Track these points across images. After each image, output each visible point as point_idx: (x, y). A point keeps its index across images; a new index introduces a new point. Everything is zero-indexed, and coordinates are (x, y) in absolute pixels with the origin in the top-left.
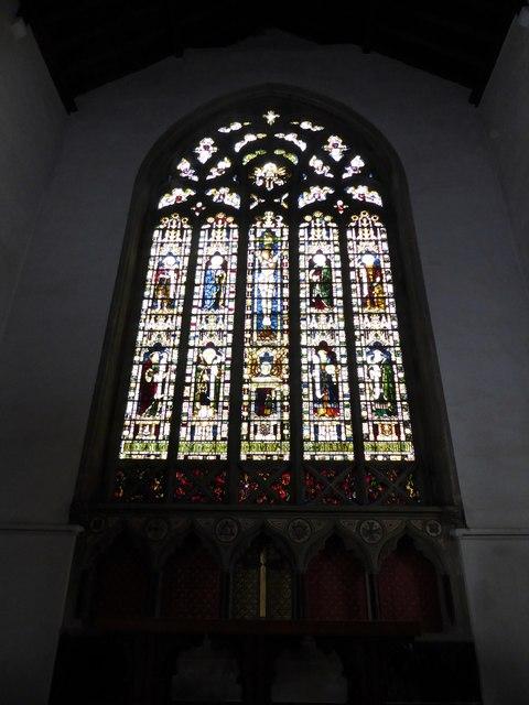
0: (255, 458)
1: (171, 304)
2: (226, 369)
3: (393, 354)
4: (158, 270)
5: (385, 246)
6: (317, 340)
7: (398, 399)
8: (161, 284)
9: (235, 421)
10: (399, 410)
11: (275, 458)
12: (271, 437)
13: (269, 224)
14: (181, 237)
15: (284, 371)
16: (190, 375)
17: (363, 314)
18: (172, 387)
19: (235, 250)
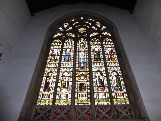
0: (80, 104)
1: (55, 61)
2: (71, 78)
3: (119, 73)
4: (52, 52)
5: (113, 46)
6: (97, 70)
7: (122, 85)
8: (53, 55)
9: (73, 93)
10: (123, 89)
11: (86, 104)
12: (84, 98)
13: (82, 41)
14: (59, 44)
15: (88, 78)
16: (60, 80)
17: (109, 62)
18: (55, 83)
19: (73, 47)
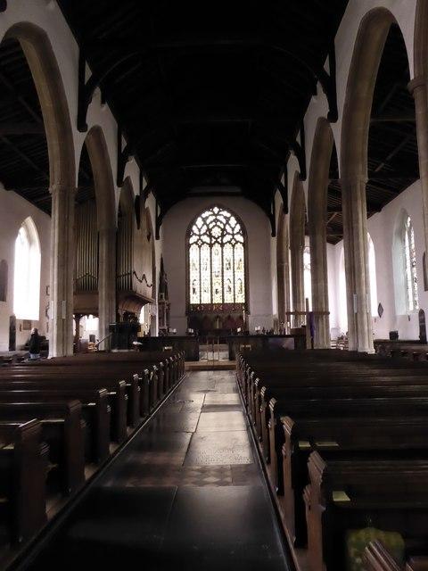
9: (212, 295)
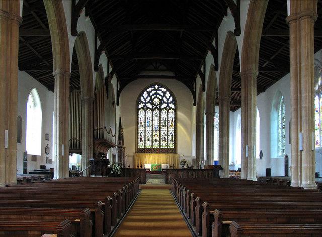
9: (153, 143)
